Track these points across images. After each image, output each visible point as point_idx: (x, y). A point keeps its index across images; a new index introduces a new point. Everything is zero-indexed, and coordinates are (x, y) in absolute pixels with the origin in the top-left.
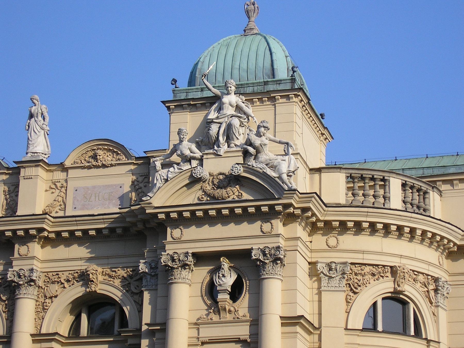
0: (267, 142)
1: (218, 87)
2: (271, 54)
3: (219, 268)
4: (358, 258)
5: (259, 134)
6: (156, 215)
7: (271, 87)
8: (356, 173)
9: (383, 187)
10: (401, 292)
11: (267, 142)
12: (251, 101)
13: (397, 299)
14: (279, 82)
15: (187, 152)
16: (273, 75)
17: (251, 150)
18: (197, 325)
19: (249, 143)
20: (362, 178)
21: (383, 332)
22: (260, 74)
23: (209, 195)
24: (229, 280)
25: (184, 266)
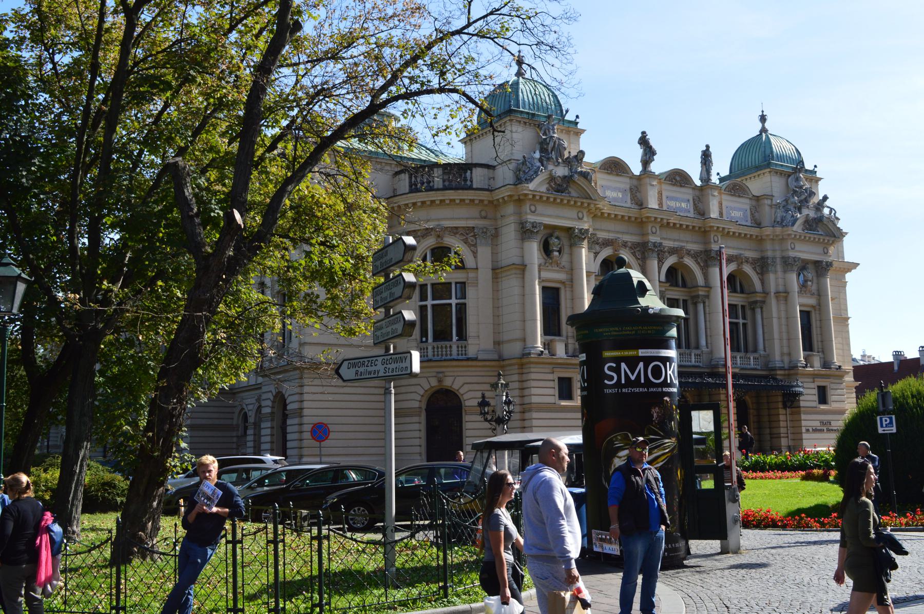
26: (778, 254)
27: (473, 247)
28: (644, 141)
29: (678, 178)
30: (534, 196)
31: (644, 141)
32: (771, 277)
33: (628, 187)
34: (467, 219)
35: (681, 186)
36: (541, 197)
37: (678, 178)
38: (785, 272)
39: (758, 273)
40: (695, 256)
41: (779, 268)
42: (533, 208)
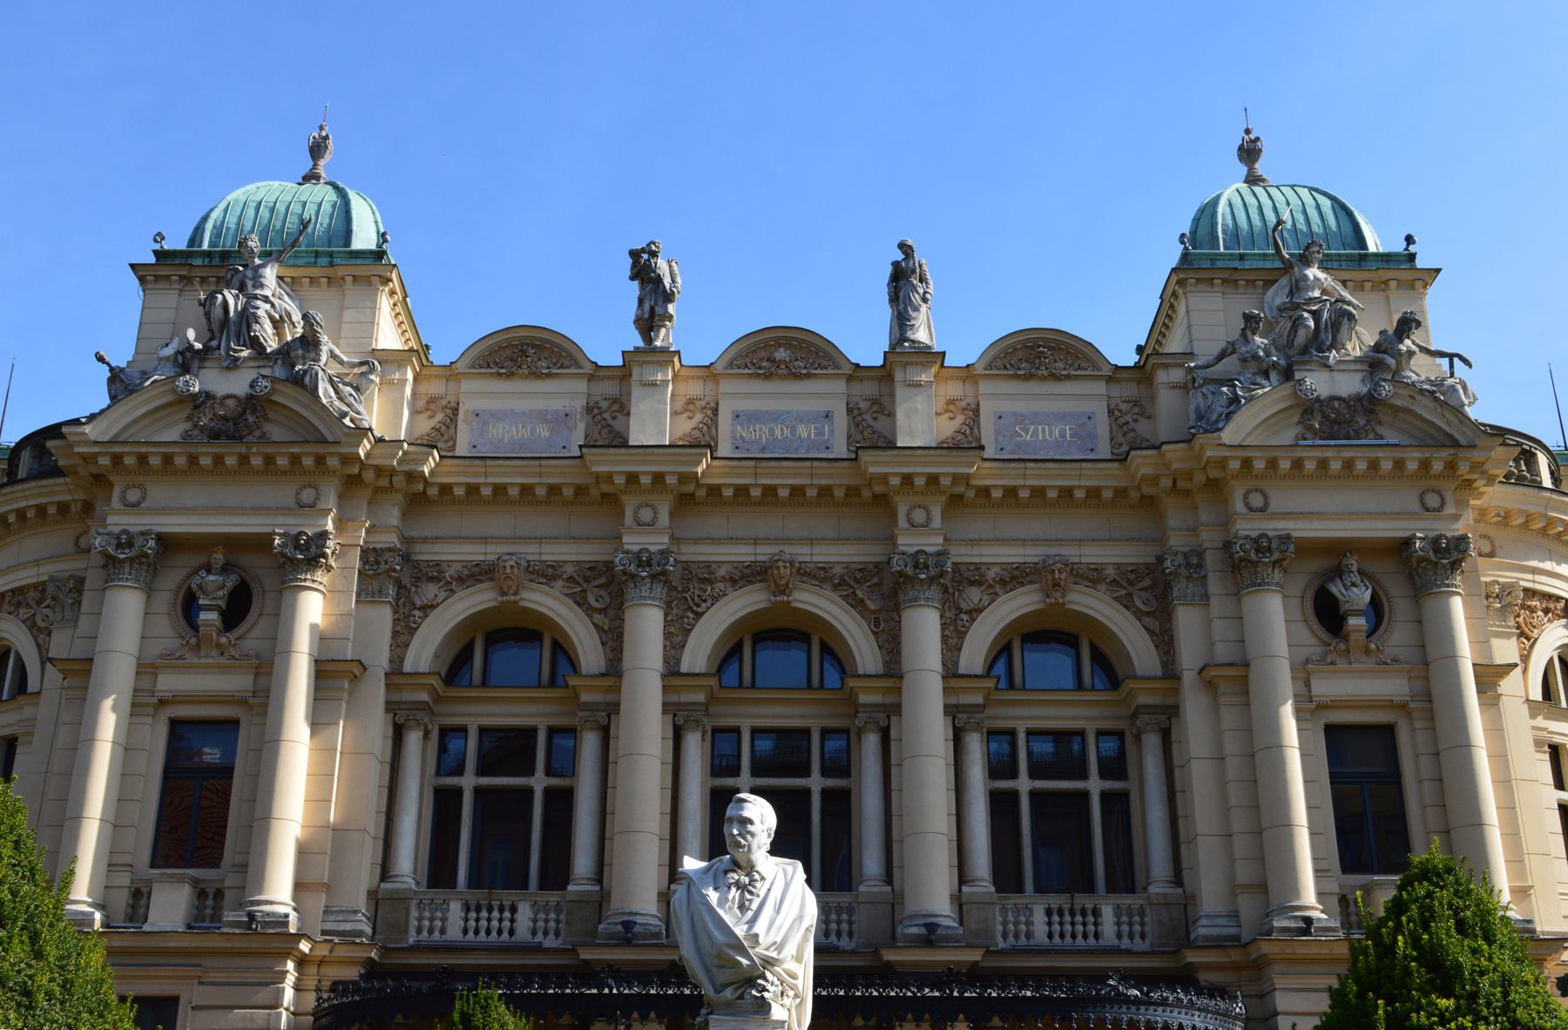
3: (1338, 572)
4: (1527, 581)
11: (1414, 348)
12: (1344, 283)
14: (1386, 258)
17: (1391, 361)
26: (1209, 538)
27: (41, 633)
28: (643, 268)
29: (785, 354)
30: (143, 459)
31: (643, 268)
32: (1186, 621)
33: (579, 404)
34: (37, 562)
35: (797, 377)
36: (168, 459)
37: (782, 354)
38: (1237, 595)
39: (1139, 614)
40: (847, 583)
41: (1216, 584)
42: (133, 495)
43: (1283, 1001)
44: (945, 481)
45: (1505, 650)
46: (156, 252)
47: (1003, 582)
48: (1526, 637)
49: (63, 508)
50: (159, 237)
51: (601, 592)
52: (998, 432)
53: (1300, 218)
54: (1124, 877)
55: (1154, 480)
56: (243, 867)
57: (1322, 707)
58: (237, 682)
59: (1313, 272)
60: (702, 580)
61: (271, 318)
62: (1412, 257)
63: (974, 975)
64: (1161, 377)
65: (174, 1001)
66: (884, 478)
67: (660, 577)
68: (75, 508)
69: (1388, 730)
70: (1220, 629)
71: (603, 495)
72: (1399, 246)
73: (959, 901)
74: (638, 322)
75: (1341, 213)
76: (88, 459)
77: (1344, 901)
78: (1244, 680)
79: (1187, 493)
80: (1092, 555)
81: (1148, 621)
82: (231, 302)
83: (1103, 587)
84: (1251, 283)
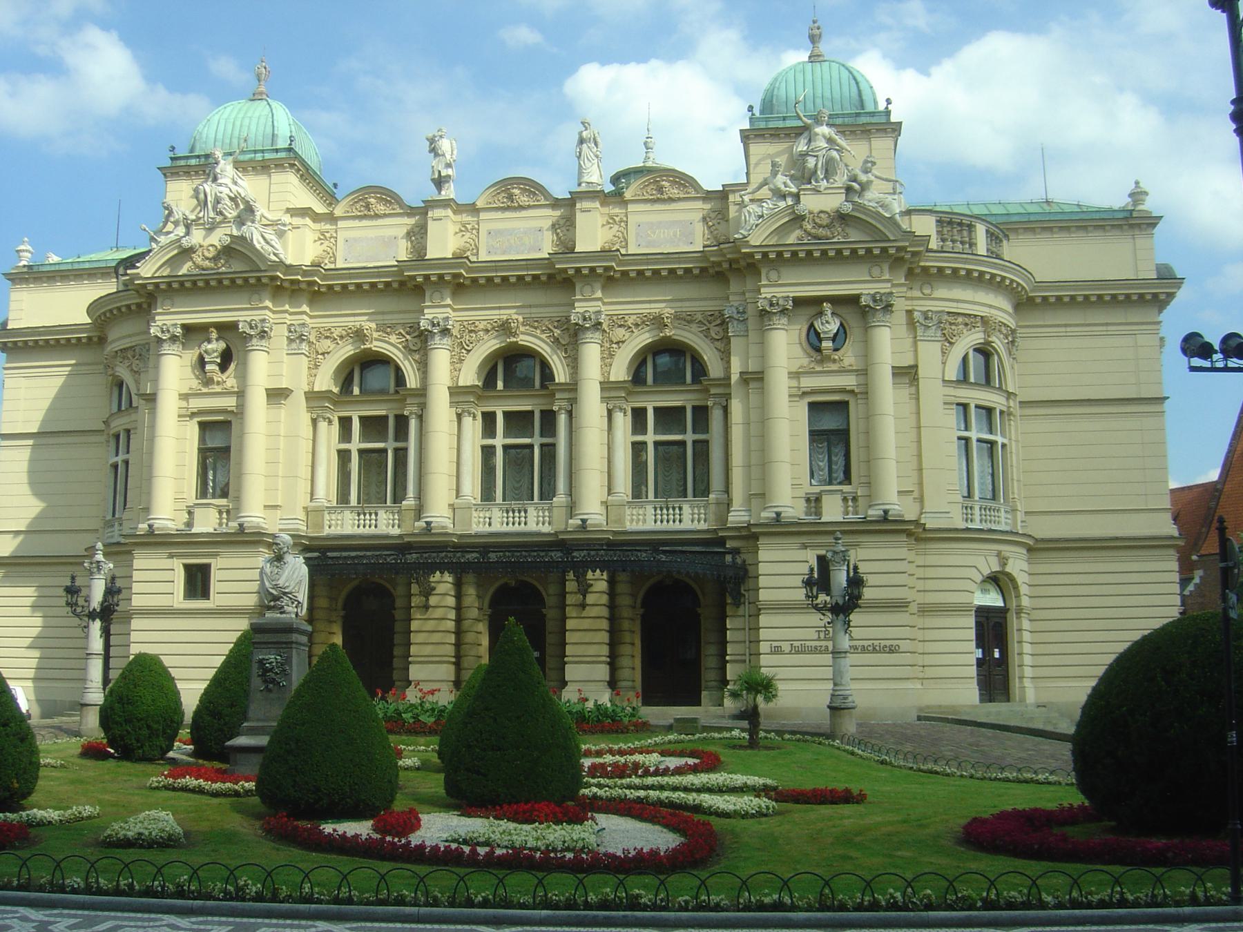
0: (873, 178)
1: (809, 117)
2: (857, 83)
3: (821, 314)
5: (866, 171)
6: (751, 255)
7: (863, 120)
8: (946, 218)
9: (970, 232)
10: (988, 343)
11: (873, 178)
12: (843, 133)
13: (985, 352)
14: (872, 114)
15: (782, 187)
16: (863, 107)
18: (795, 375)
19: (854, 179)
20: (950, 223)
21: (975, 384)
22: (846, 104)
23: (809, 234)
24: (833, 326)
25: (784, 311)
32: (736, 344)
34: (130, 336)
41: (752, 323)
43: (763, 555)
44: (599, 271)
45: (929, 355)
46: (172, 159)
47: (637, 325)
48: (949, 340)
49: (139, 306)
50: (173, 149)
51: (416, 340)
52: (637, 234)
53: (827, 88)
54: (702, 489)
55: (719, 264)
56: (238, 499)
57: (804, 393)
58: (230, 402)
59: (818, 130)
60: (471, 331)
61: (231, 198)
62: (887, 113)
63: (611, 545)
64: (731, 198)
65: (208, 566)
66: (565, 270)
67: (445, 332)
68: (145, 306)
69: (847, 403)
70: (754, 350)
71: (415, 286)
72: (882, 106)
73: (605, 504)
74: (433, 180)
75: (853, 82)
76: (144, 286)
77: (808, 500)
78: (762, 379)
79: (738, 270)
80: (688, 307)
81: (718, 344)
82: (208, 190)
83: (694, 328)
84: (787, 135)
